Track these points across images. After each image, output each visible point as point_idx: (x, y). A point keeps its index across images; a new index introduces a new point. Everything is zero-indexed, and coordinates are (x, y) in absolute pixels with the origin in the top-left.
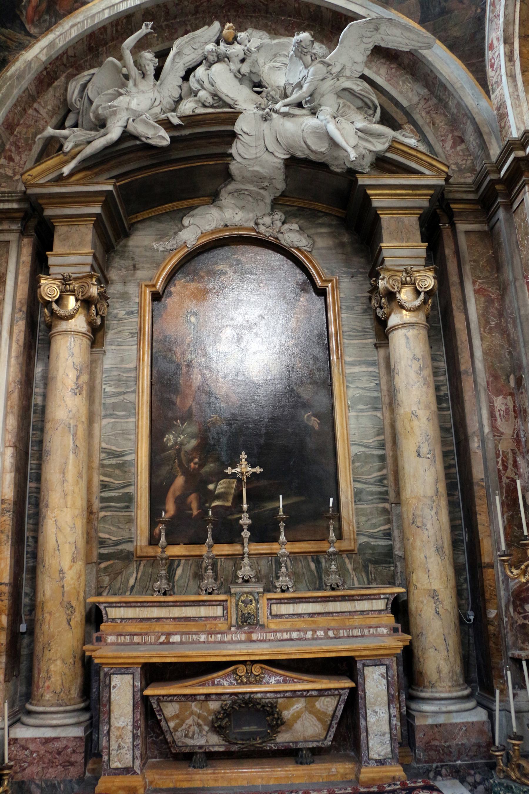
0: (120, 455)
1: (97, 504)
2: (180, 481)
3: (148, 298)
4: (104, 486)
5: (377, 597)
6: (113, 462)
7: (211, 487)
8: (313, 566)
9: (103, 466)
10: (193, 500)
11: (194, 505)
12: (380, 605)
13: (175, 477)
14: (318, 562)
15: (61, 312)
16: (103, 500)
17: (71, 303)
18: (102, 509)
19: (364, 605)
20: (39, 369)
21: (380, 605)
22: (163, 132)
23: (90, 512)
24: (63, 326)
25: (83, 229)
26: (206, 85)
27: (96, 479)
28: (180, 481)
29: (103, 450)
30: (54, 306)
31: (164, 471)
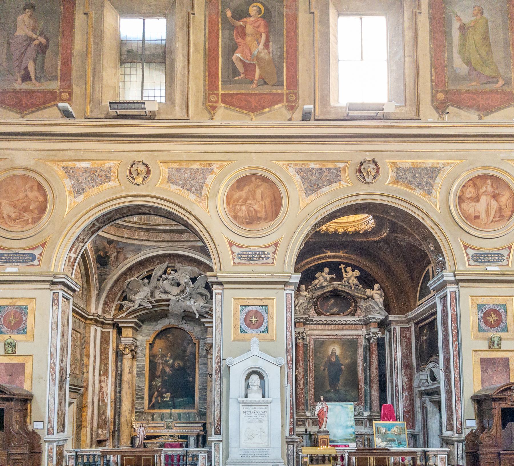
0: (141, 387)
1: (135, 399)
2: (156, 393)
3: (148, 345)
4: (137, 395)
5: (199, 423)
6: (139, 389)
7: (164, 395)
8: (187, 415)
9: (136, 390)
10: (159, 399)
11: (159, 400)
12: (200, 425)
13: (155, 393)
14: (189, 415)
15: (125, 353)
16: (136, 398)
17: (127, 350)
18: (136, 400)
19: (196, 425)
20: (119, 364)
21: (200, 425)
22: (150, 305)
23: (133, 401)
24: (125, 356)
25: (130, 329)
26: (162, 287)
27: (135, 393)
28: (156, 393)
29: (136, 386)
30: (123, 351)
31: (152, 391)
